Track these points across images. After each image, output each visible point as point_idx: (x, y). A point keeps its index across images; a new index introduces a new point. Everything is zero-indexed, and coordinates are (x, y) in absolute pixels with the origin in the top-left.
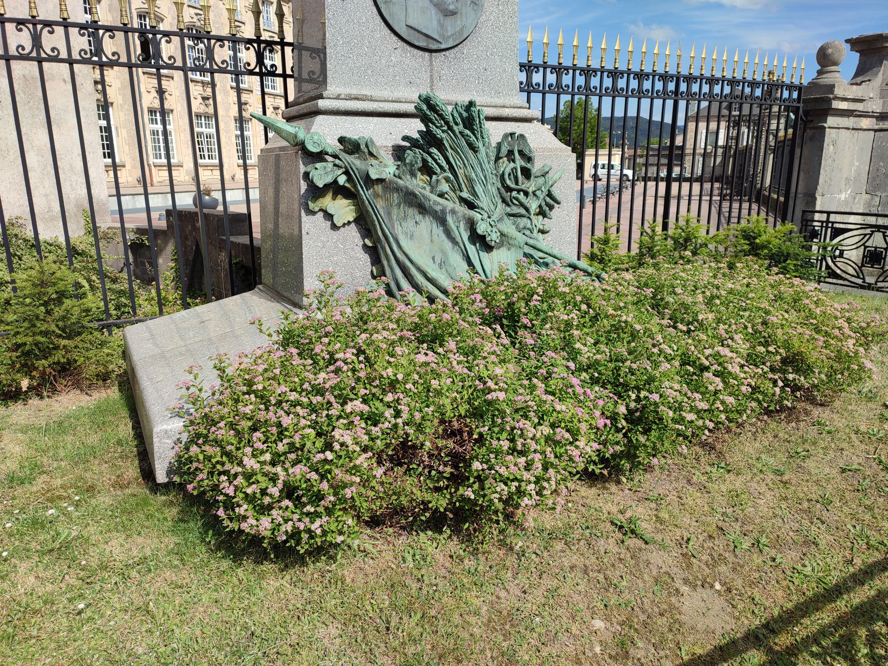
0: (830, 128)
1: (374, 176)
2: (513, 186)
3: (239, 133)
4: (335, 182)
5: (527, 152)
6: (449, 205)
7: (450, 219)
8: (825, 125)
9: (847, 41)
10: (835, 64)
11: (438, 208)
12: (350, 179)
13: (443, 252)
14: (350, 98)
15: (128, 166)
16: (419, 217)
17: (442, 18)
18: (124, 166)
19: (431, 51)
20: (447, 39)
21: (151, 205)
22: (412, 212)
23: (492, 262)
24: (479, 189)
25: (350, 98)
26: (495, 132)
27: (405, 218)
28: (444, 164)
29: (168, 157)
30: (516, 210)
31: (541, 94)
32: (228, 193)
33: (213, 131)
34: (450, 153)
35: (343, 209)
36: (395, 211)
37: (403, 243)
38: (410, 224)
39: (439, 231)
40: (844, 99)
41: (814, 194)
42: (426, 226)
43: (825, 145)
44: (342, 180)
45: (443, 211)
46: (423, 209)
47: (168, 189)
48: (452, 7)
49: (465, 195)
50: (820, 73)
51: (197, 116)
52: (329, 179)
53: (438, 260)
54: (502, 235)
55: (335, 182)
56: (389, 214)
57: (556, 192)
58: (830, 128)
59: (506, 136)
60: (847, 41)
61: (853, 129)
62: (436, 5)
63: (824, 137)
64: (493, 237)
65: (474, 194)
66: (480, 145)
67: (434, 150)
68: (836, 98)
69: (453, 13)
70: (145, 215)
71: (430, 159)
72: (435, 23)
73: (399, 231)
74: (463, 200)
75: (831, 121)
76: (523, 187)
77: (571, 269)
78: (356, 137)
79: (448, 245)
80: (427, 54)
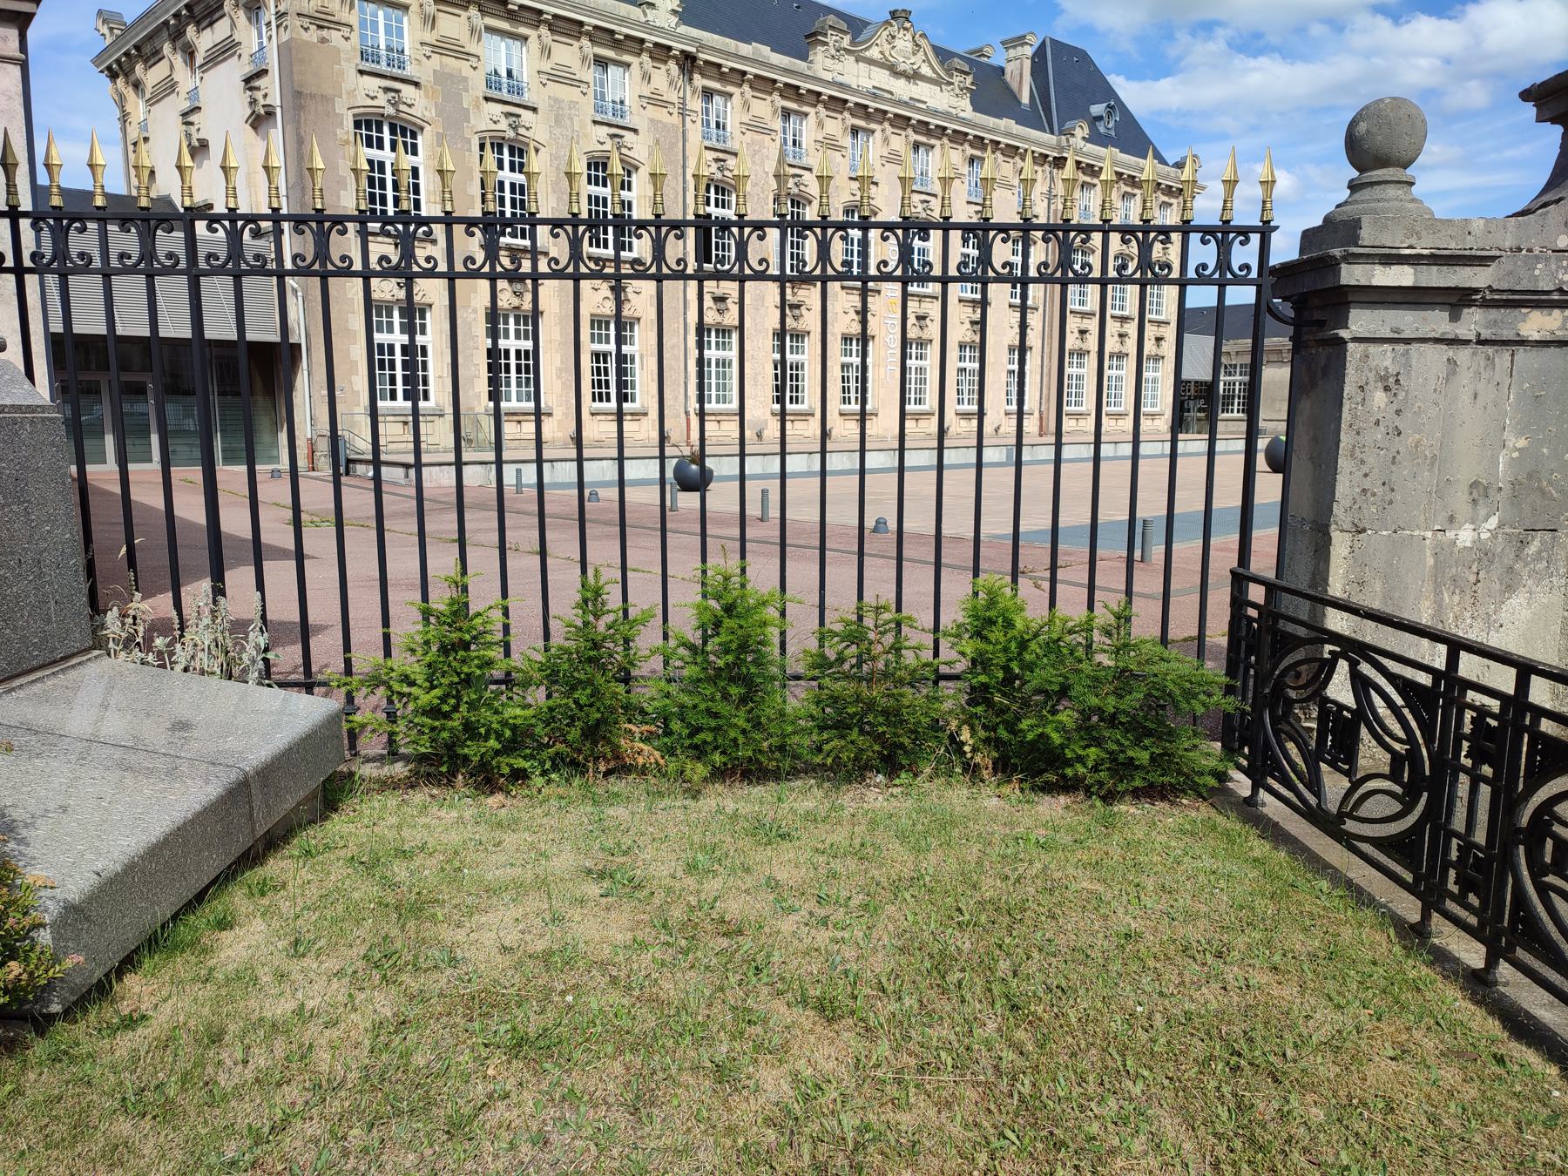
0: (1356, 340)
3: (777, 356)
8: (1344, 334)
9: (1526, 95)
15: (558, 413)
18: (550, 415)
21: (788, 470)
29: (623, 398)
31: (360, 280)
32: (868, 455)
33: (733, 354)
40: (1391, 259)
41: (1328, 526)
43: (1349, 388)
47: (777, 449)
50: (1354, 187)
51: (792, 336)
58: (1356, 340)
60: (1526, 95)
61: (1482, 342)
63: (1344, 367)
68: (1352, 259)
70: (575, 492)
75: (1361, 321)
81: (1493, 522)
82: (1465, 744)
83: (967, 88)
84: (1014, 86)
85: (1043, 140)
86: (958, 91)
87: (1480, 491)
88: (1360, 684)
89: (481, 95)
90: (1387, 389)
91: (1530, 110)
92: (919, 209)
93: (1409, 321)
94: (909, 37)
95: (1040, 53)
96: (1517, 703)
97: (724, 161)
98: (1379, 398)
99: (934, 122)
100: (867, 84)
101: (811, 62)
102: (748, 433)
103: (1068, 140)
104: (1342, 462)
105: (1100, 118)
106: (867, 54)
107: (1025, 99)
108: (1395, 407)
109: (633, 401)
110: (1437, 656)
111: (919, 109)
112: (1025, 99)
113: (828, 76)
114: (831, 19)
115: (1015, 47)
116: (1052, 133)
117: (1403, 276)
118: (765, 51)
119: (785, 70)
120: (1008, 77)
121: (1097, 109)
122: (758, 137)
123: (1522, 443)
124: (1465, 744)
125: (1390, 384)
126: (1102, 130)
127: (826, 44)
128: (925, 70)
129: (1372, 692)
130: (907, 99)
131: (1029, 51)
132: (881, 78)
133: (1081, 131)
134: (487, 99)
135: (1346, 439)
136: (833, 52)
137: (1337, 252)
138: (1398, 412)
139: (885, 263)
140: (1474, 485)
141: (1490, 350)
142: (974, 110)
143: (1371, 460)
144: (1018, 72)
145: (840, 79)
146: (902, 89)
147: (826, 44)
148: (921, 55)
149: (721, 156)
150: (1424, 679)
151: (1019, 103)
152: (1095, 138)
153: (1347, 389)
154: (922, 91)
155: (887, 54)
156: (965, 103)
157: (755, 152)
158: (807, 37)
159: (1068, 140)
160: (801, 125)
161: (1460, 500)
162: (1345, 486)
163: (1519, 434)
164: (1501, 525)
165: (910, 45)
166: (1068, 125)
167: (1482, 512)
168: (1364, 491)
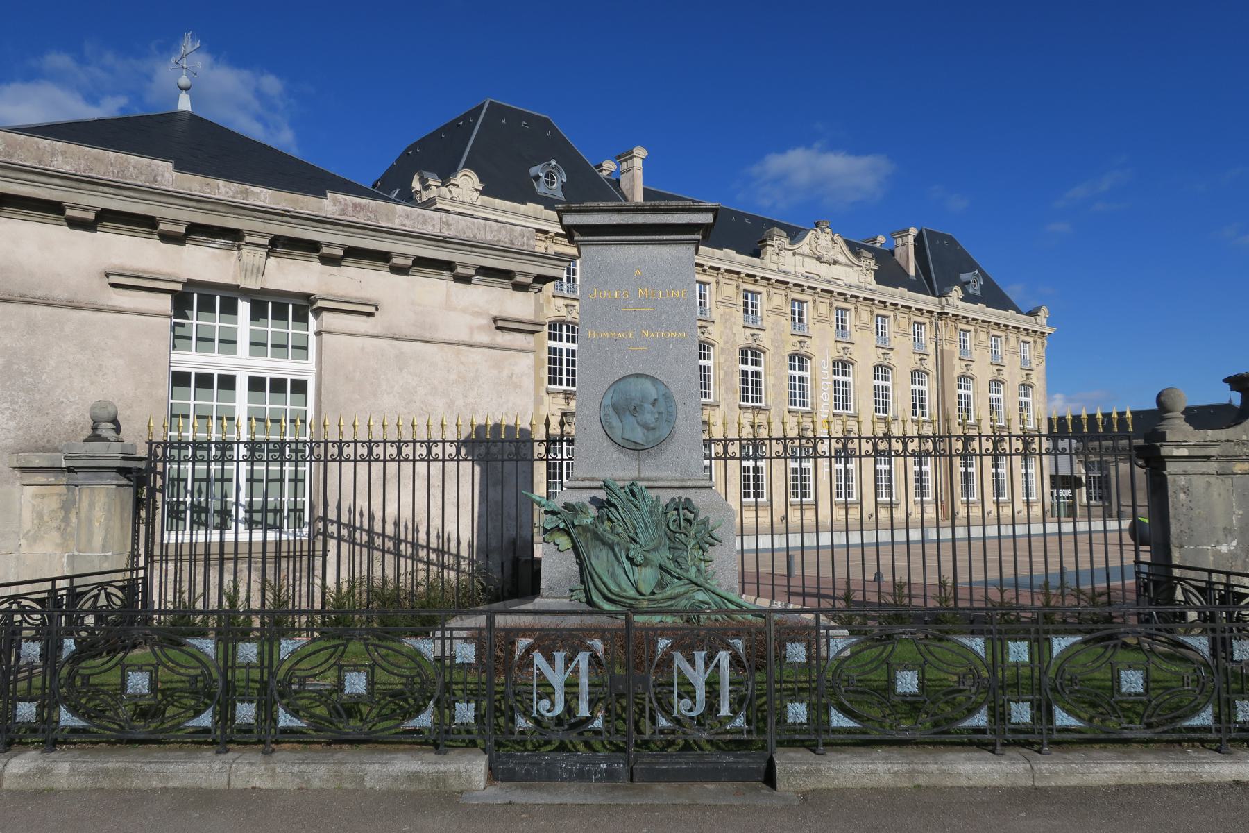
1: (576, 523)
2: (678, 530)
4: (558, 526)
5: (691, 509)
6: (616, 539)
7: (616, 549)
9: (1225, 381)
10: (1169, 411)
11: (610, 542)
12: (566, 525)
13: (613, 567)
14: (584, 479)
16: (601, 547)
17: (646, 431)
19: (639, 450)
20: (648, 443)
22: (599, 543)
23: (640, 574)
24: (639, 532)
25: (584, 479)
26: (666, 497)
27: (595, 547)
28: (619, 517)
30: (676, 545)
34: (620, 510)
35: (564, 541)
36: (590, 543)
37: (593, 562)
38: (598, 550)
39: (611, 555)
42: (605, 553)
43: (1170, 493)
44: (562, 525)
45: (613, 543)
46: (604, 543)
48: (652, 425)
49: (631, 535)
52: (553, 525)
53: (610, 572)
54: (646, 558)
55: (558, 526)
56: (587, 545)
57: (715, 534)
59: (673, 499)
60: (1225, 381)
62: (641, 425)
64: (639, 560)
65: (637, 534)
66: (643, 506)
67: (612, 509)
69: (653, 429)
71: (610, 514)
72: (641, 435)
73: (591, 553)
74: (629, 537)
76: (684, 531)
77: (688, 582)
78: (573, 502)
79: (616, 563)
80: (636, 452)
81: (1235, 543)
82: (1217, 601)
83: (872, 269)
84: (903, 263)
85: (927, 302)
86: (864, 271)
87: (1228, 531)
88: (1185, 591)
89: (551, 295)
90: (1185, 493)
91: (1227, 386)
92: (842, 354)
93: (1188, 466)
94: (829, 237)
95: (919, 239)
96: (1228, 586)
97: (706, 327)
98: (1182, 496)
99: (850, 292)
100: (801, 270)
101: (763, 258)
102: (775, 519)
103: (947, 300)
104: (1172, 521)
105: (968, 283)
106: (800, 251)
107: (912, 272)
108: (1189, 499)
109: (762, 497)
110: (1205, 576)
111: (839, 285)
112: (912, 272)
113: (774, 267)
114: (776, 230)
115: (901, 237)
116: (934, 295)
117: (1184, 452)
118: (732, 253)
119: (747, 265)
120: (897, 257)
121: (964, 277)
122: (728, 310)
123: (1241, 512)
124: (1217, 601)
125: (1186, 490)
126: (971, 291)
127: (773, 246)
128: (841, 258)
129: (1190, 595)
130: (829, 279)
131: (911, 239)
132: (812, 266)
133: (956, 292)
134: (554, 296)
135: (1171, 511)
136: (778, 251)
137: (1158, 444)
138: (1190, 501)
139: (988, 450)
140: (1225, 528)
141: (1222, 477)
142: (877, 283)
143: (1182, 519)
144: (904, 255)
145: (783, 268)
146: (824, 270)
147: (773, 246)
148: (838, 249)
149: (704, 324)
150: (1204, 585)
151: (908, 275)
152: (968, 298)
153: (1169, 494)
154: (836, 271)
155: (814, 250)
156: (870, 278)
157: (726, 321)
158: (759, 242)
159: (947, 300)
160: (756, 300)
161: (1220, 534)
162: (1174, 529)
163: (1239, 509)
164: (1238, 544)
165: (830, 243)
166: (946, 290)
167: (1230, 539)
168: (1182, 531)
